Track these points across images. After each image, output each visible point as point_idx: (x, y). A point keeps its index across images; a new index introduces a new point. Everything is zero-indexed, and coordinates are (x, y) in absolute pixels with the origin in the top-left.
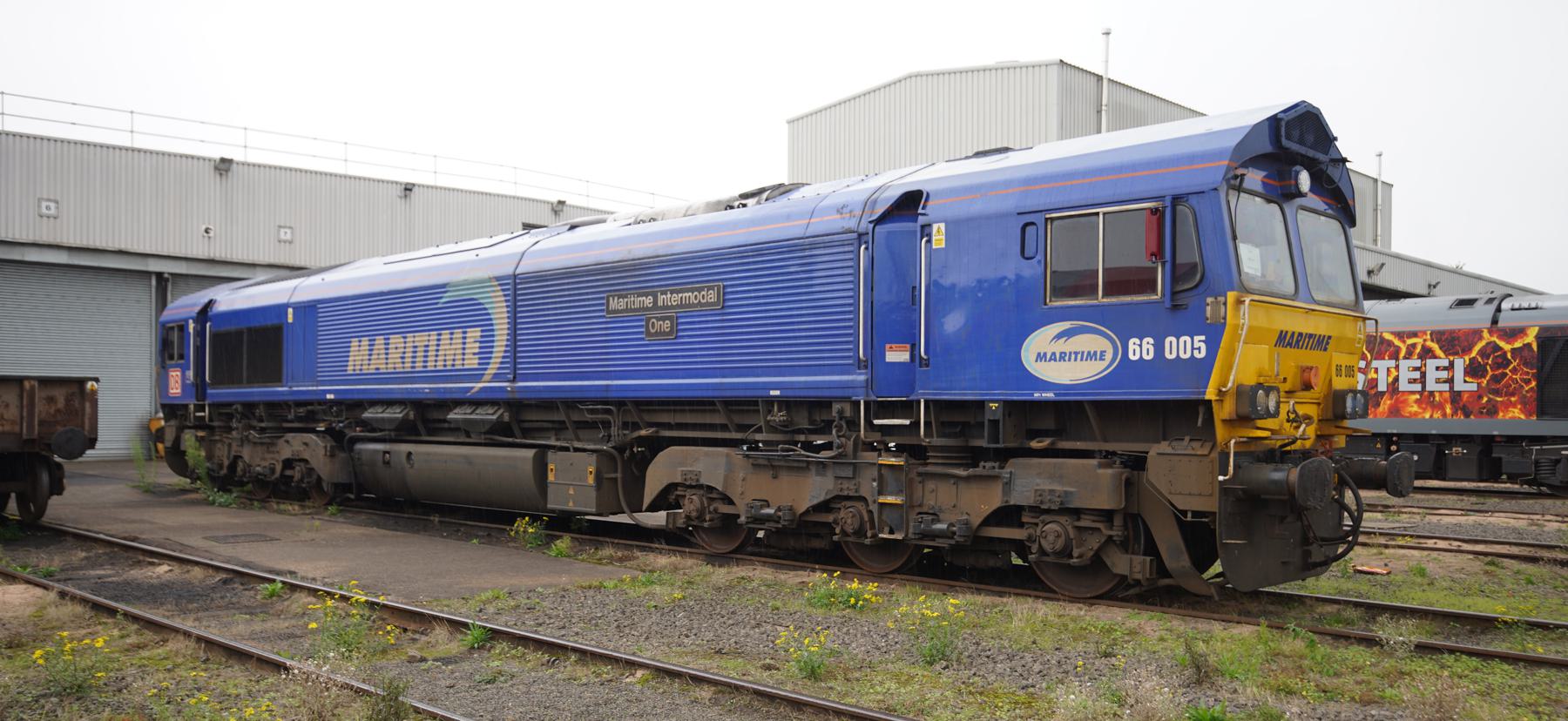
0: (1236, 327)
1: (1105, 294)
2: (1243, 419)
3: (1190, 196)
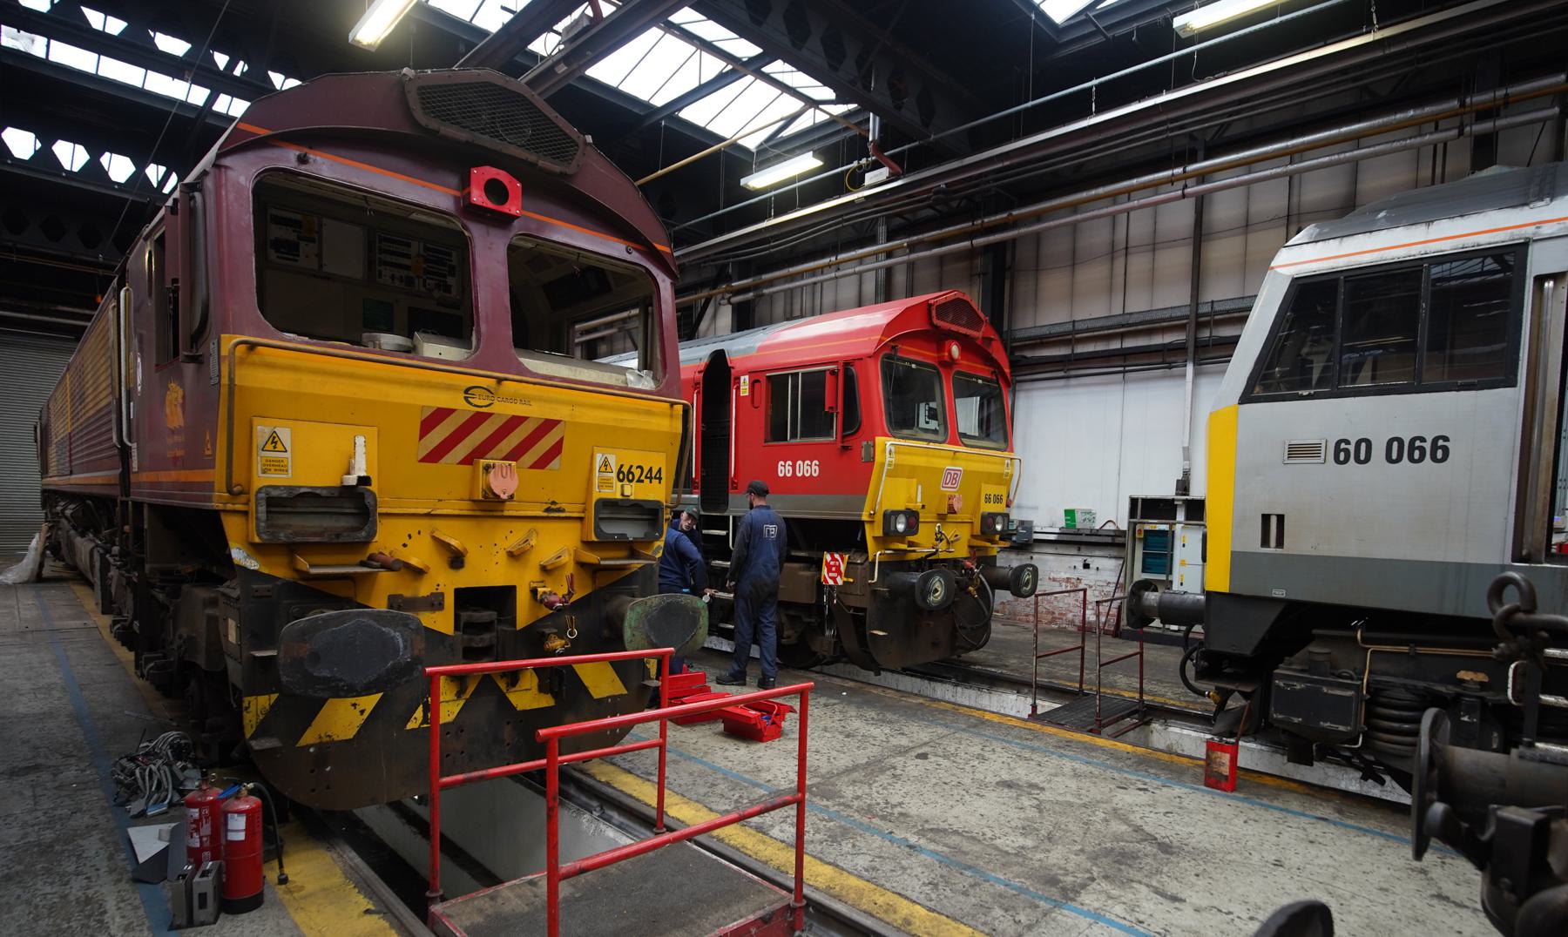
0: (883, 464)
1: (802, 436)
2: (889, 535)
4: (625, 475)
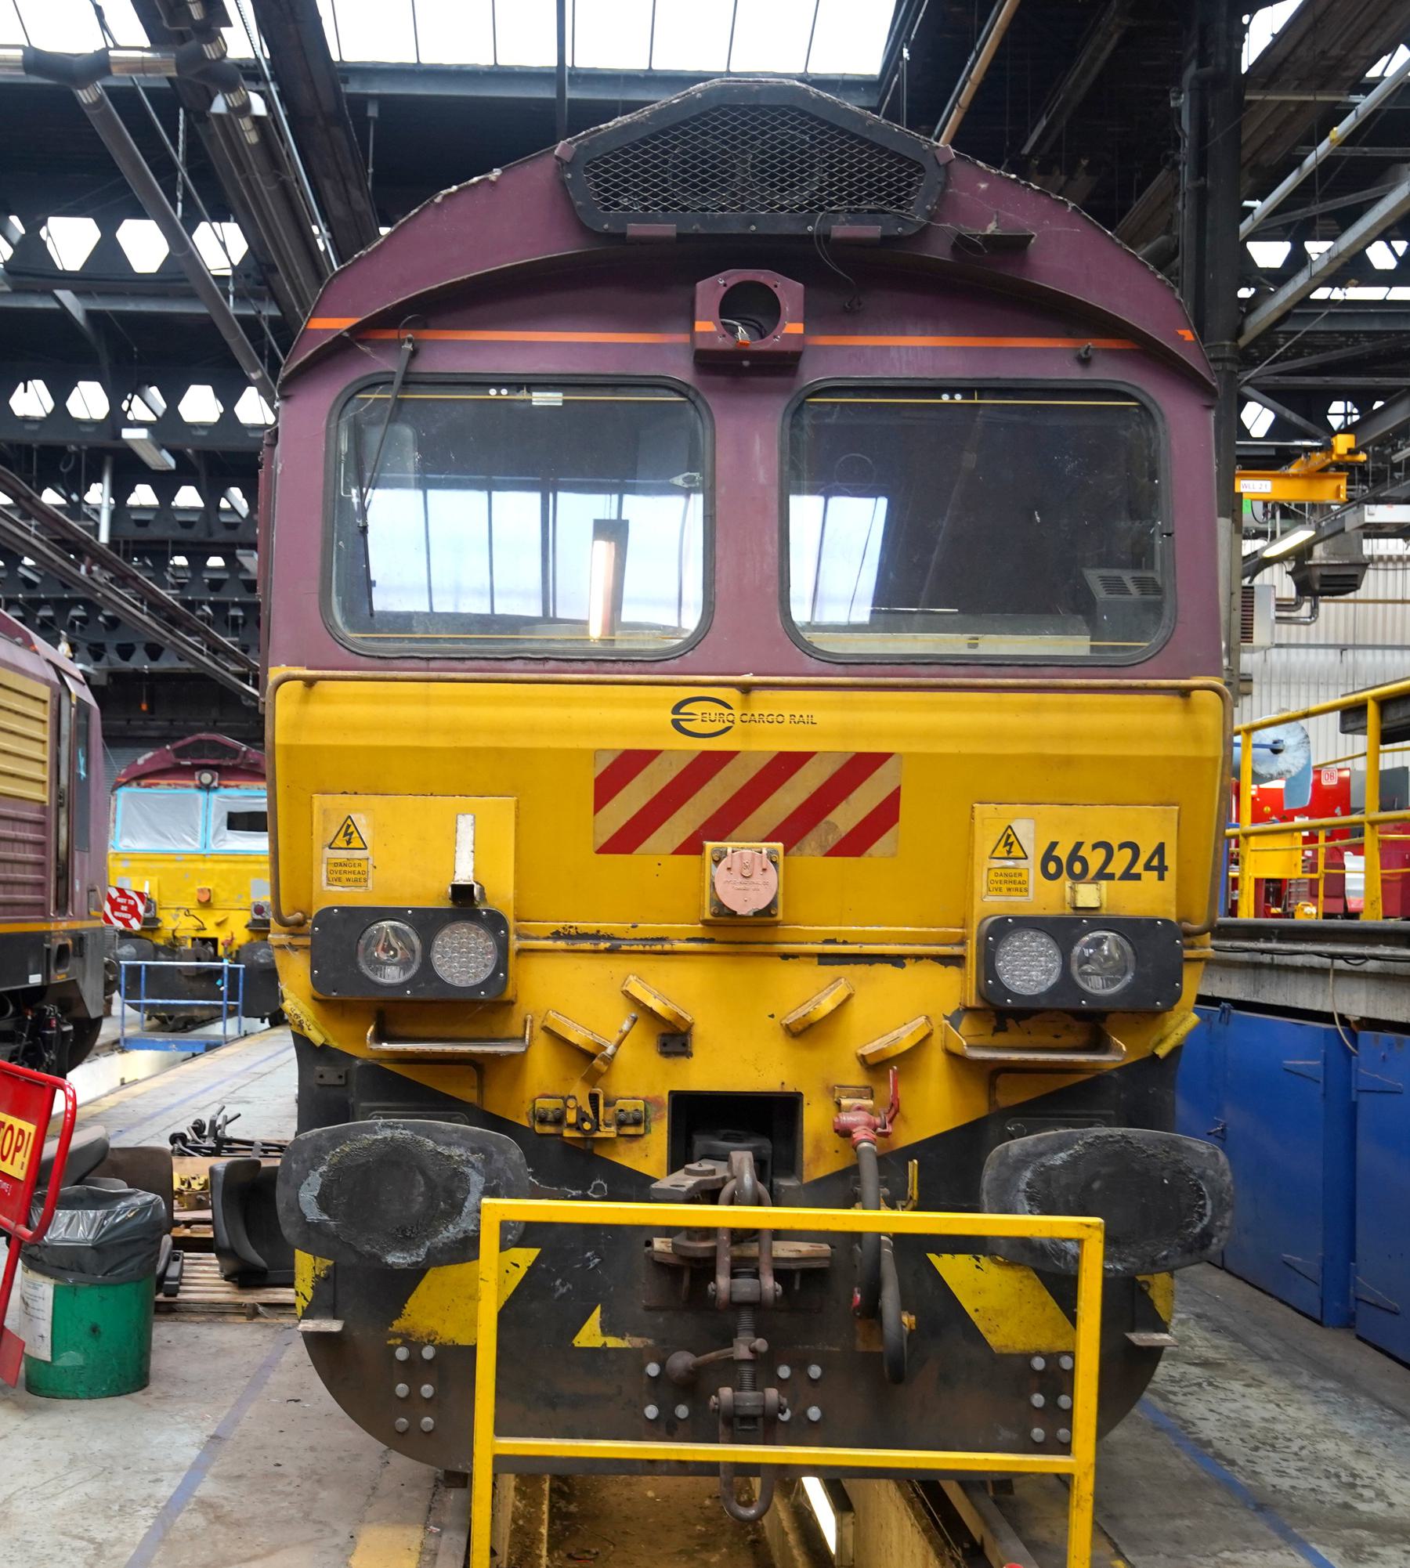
4: (1052, 864)
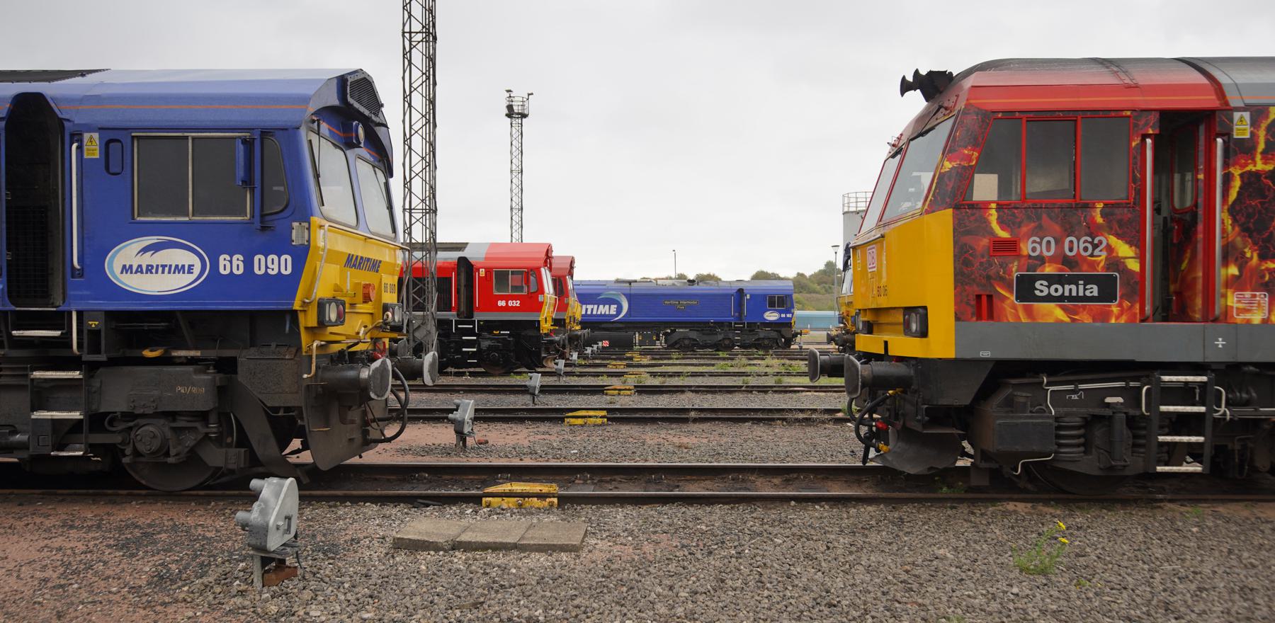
3: (276, 132)
